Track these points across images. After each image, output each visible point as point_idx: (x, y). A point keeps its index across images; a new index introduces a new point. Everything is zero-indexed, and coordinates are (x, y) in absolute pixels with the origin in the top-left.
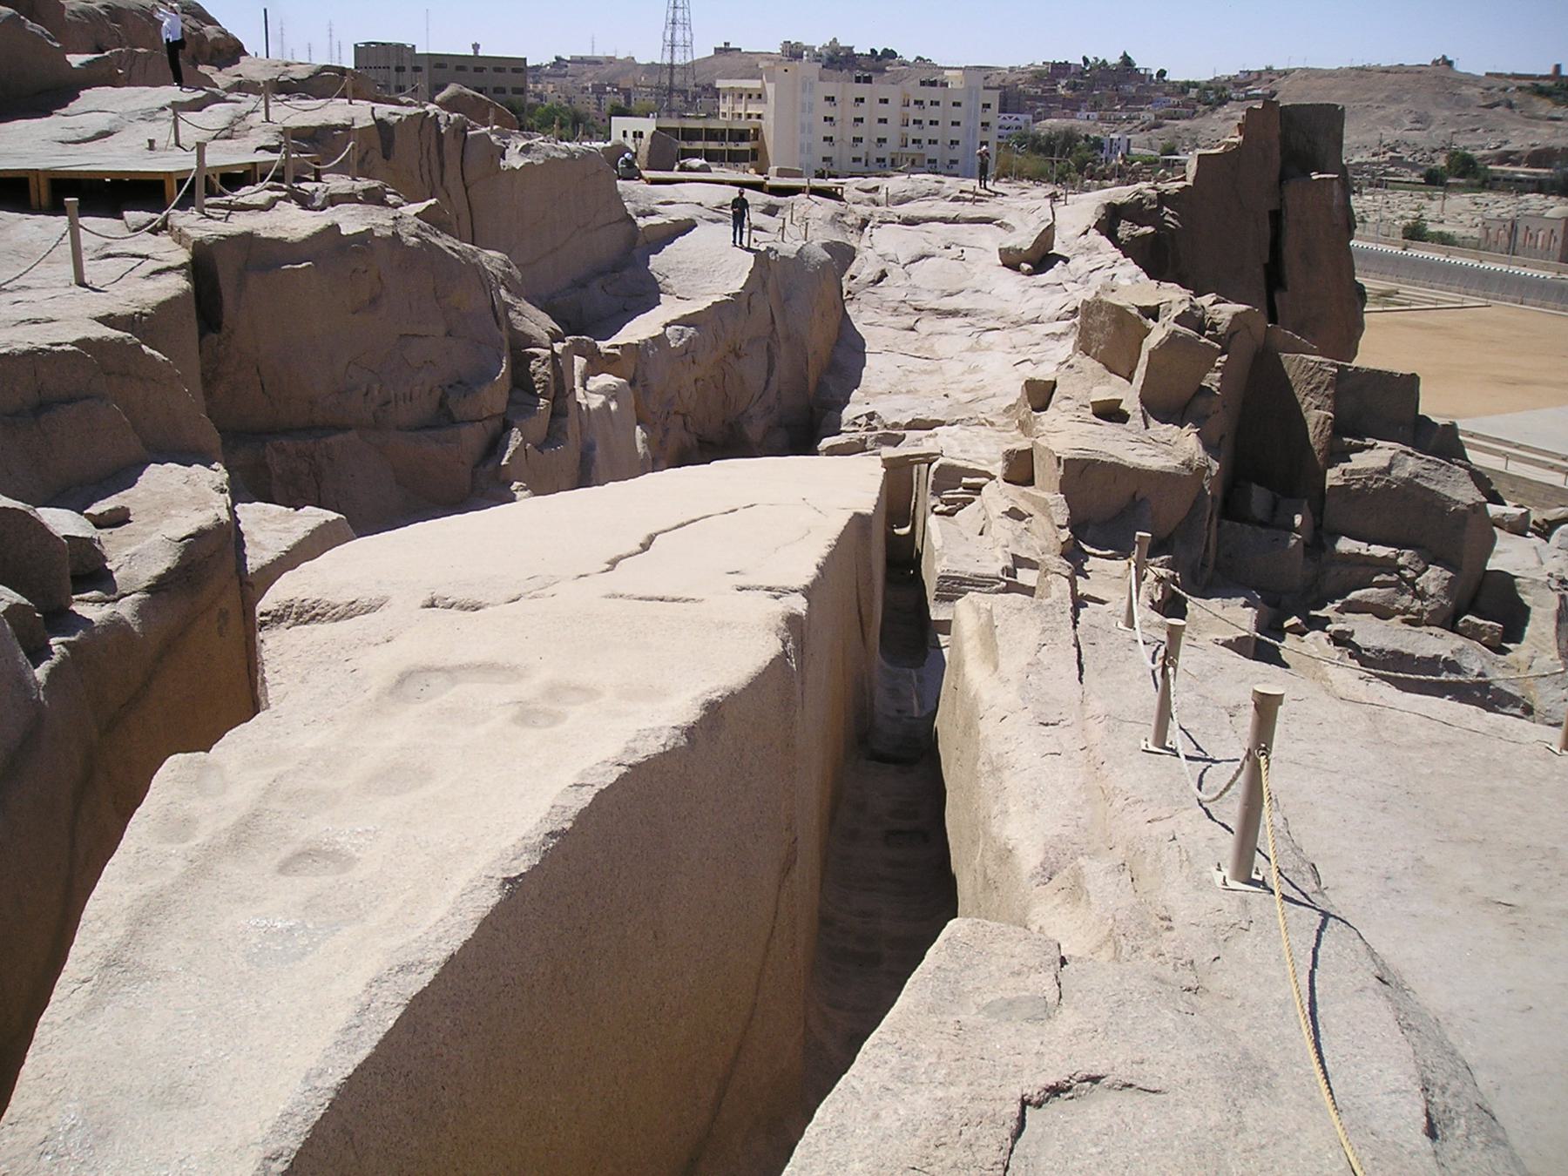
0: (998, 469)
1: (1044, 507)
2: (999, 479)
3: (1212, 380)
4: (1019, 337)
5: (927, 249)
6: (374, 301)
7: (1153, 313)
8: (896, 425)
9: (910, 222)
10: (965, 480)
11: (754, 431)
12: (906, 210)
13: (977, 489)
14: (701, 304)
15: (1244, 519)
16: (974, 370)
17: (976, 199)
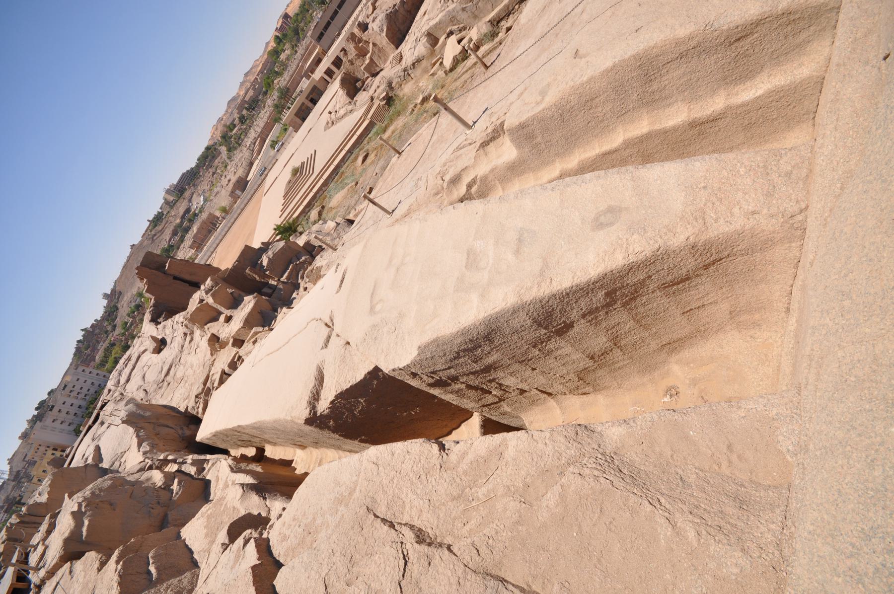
0: (235, 349)
1: (256, 333)
3: (230, 291)
4: (185, 352)
5: (141, 376)
6: (111, 504)
7: (201, 301)
8: (203, 389)
9: (128, 381)
11: (188, 432)
12: (123, 381)
13: (240, 357)
14: (135, 440)
16: (192, 366)
17: (129, 359)
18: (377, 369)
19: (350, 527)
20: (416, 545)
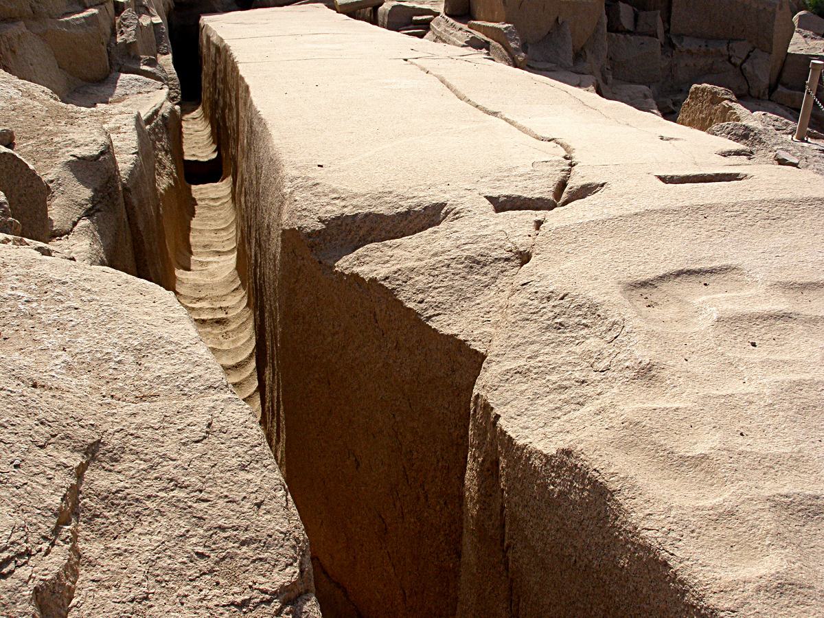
2: (443, 14)
10: (414, 18)
13: (426, 26)
15: (617, 31)
18: (477, 360)
19: (41, 415)
20: (27, 592)
